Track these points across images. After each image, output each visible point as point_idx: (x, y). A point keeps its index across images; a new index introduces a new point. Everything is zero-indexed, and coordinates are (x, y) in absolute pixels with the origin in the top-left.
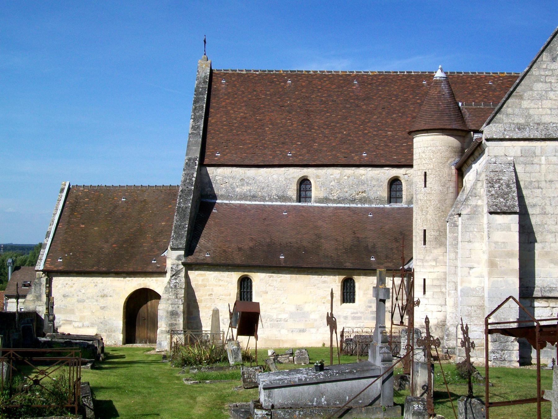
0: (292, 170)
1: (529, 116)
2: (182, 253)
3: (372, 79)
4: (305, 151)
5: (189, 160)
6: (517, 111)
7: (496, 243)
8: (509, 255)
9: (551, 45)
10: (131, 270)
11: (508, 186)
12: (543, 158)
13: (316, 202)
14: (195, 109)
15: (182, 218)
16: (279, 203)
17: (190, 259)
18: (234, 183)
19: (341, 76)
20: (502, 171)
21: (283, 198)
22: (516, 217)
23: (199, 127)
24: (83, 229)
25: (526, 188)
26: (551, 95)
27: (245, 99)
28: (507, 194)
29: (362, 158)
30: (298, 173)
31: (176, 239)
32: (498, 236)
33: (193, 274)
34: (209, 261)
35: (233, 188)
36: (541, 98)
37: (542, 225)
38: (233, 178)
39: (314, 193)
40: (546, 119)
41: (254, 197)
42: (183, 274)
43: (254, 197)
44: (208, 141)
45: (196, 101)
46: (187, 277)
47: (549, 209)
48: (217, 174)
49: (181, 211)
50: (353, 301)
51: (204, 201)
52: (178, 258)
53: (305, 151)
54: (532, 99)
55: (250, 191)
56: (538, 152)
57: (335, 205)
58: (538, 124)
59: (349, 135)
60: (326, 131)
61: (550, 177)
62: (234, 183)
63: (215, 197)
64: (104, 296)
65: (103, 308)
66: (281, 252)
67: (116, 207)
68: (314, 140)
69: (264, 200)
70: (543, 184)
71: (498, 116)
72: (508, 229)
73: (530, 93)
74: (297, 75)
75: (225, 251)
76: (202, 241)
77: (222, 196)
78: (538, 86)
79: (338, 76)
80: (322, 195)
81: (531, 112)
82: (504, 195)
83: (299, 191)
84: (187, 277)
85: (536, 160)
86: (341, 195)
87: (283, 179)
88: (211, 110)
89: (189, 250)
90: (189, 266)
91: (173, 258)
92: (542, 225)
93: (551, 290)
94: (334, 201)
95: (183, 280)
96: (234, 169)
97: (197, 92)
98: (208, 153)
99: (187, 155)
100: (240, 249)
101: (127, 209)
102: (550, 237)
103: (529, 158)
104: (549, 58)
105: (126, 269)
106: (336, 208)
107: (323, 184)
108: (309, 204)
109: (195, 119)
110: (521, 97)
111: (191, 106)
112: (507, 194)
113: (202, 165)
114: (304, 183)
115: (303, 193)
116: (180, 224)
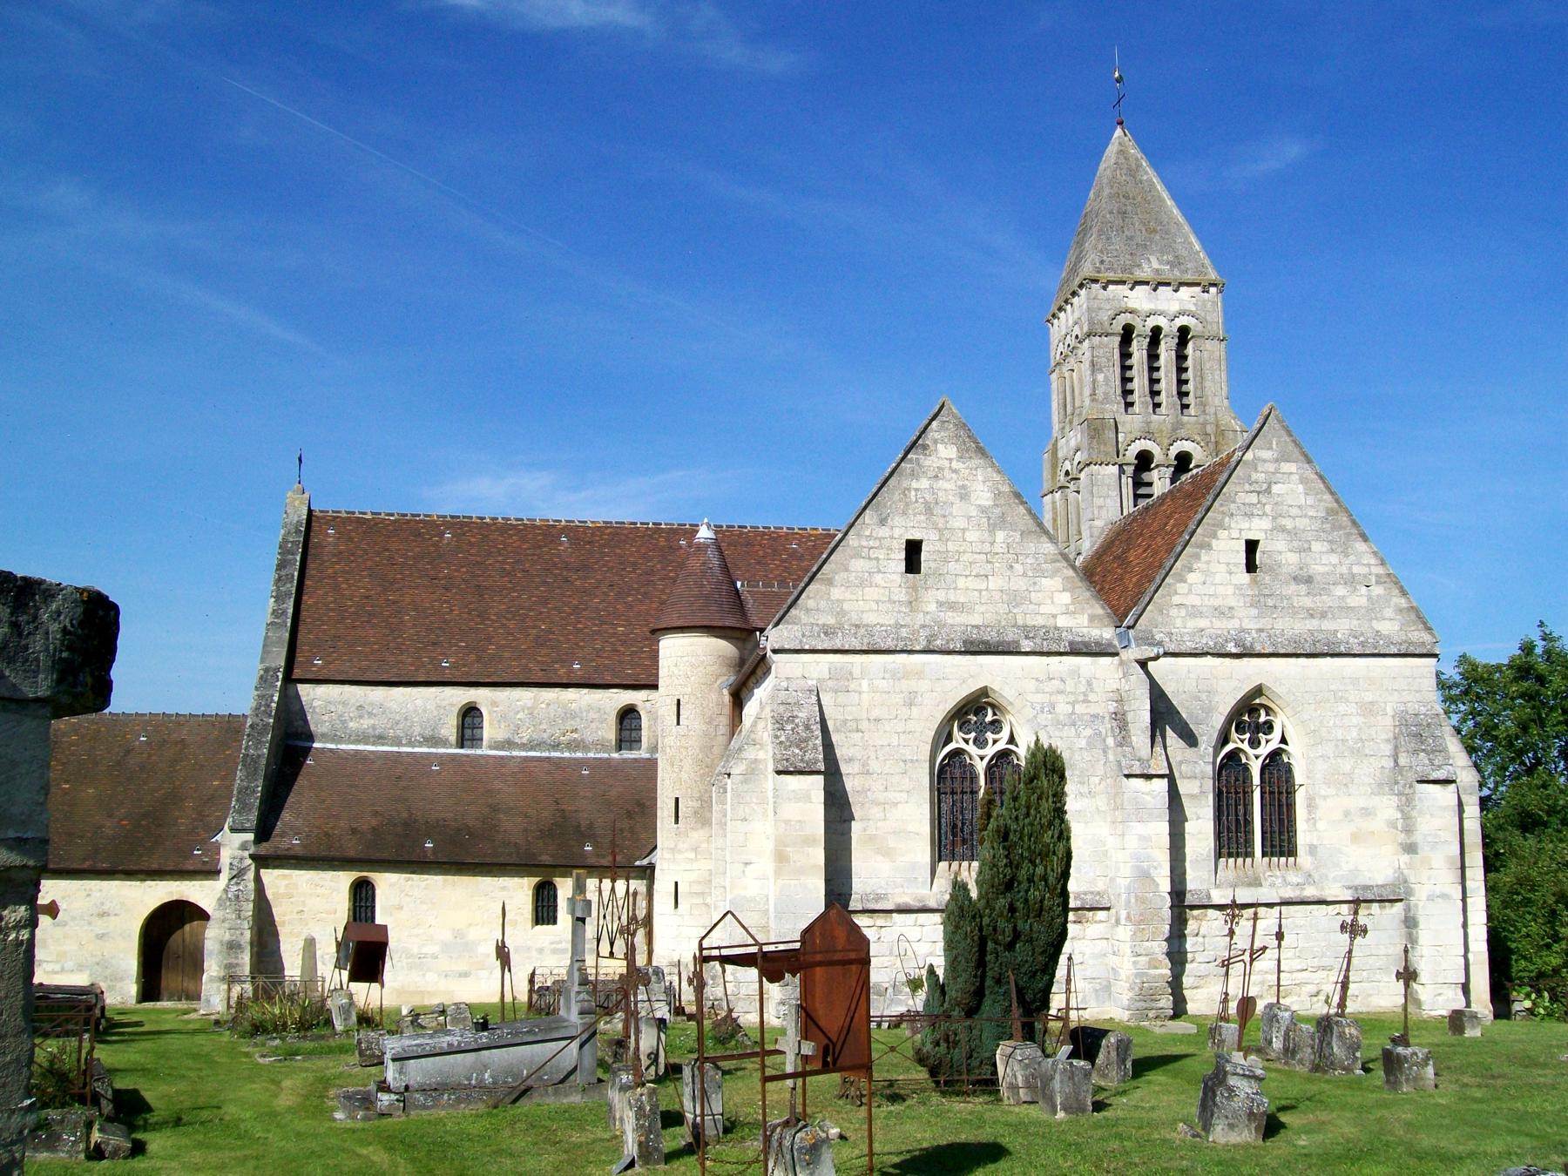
0: (449, 691)
1: (843, 613)
2: (251, 836)
3: (593, 534)
4: (473, 657)
5: (266, 670)
6: (823, 604)
7: (787, 822)
8: (809, 841)
9: (878, 498)
10: (155, 866)
11: (807, 727)
12: (865, 683)
13: (491, 747)
14: (279, 579)
15: (250, 776)
16: (424, 750)
17: (265, 848)
18: (344, 713)
19: (539, 528)
20: (797, 704)
23: (284, 612)
24: (65, 792)
25: (838, 731)
26: (878, 578)
27: (369, 563)
28: (806, 740)
29: (572, 671)
30: (459, 697)
31: (239, 812)
32: (791, 811)
33: (268, 875)
34: (300, 852)
36: (862, 584)
37: (864, 791)
38: (345, 704)
39: (489, 732)
40: (870, 618)
41: (380, 739)
42: (251, 875)
43: (380, 739)
44: (300, 636)
45: (281, 566)
46: (258, 880)
47: (874, 766)
48: (312, 695)
49: (251, 763)
50: (555, 923)
51: (291, 743)
52: (244, 847)
53: (473, 657)
54: (847, 585)
56: (856, 672)
57: (524, 754)
58: (857, 626)
59: (550, 631)
60: (511, 624)
61: (875, 713)
62: (344, 713)
63: (310, 737)
64: (103, 915)
65: (101, 937)
66: (429, 836)
67: (128, 752)
68: (489, 639)
69: (399, 744)
70: (864, 725)
71: (793, 612)
72: (808, 798)
73: (845, 575)
74: (463, 524)
75: (327, 834)
76: (286, 816)
77: (323, 735)
78: (858, 565)
79: (535, 527)
80: (501, 735)
81: (846, 606)
82: (801, 743)
83: (462, 727)
84: (258, 880)
85: (852, 686)
87: (434, 707)
88: (307, 582)
89: (263, 832)
90: (262, 861)
91: (232, 845)
92: (864, 791)
93: (878, 898)
94: (523, 747)
95: (251, 885)
96: (347, 688)
97: (284, 549)
98: (299, 658)
99: (262, 661)
100: (354, 831)
101: (150, 756)
102: (875, 812)
103: (842, 682)
104: (876, 519)
105: (145, 866)
106: (526, 759)
107: (504, 717)
108: (479, 752)
109: (279, 598)
110: (830, 582)
111: (272, 575)
112: (806, 740)
113: (290, 679)
114: (470, 714)
115: (468, 732)
116: (249, 785)
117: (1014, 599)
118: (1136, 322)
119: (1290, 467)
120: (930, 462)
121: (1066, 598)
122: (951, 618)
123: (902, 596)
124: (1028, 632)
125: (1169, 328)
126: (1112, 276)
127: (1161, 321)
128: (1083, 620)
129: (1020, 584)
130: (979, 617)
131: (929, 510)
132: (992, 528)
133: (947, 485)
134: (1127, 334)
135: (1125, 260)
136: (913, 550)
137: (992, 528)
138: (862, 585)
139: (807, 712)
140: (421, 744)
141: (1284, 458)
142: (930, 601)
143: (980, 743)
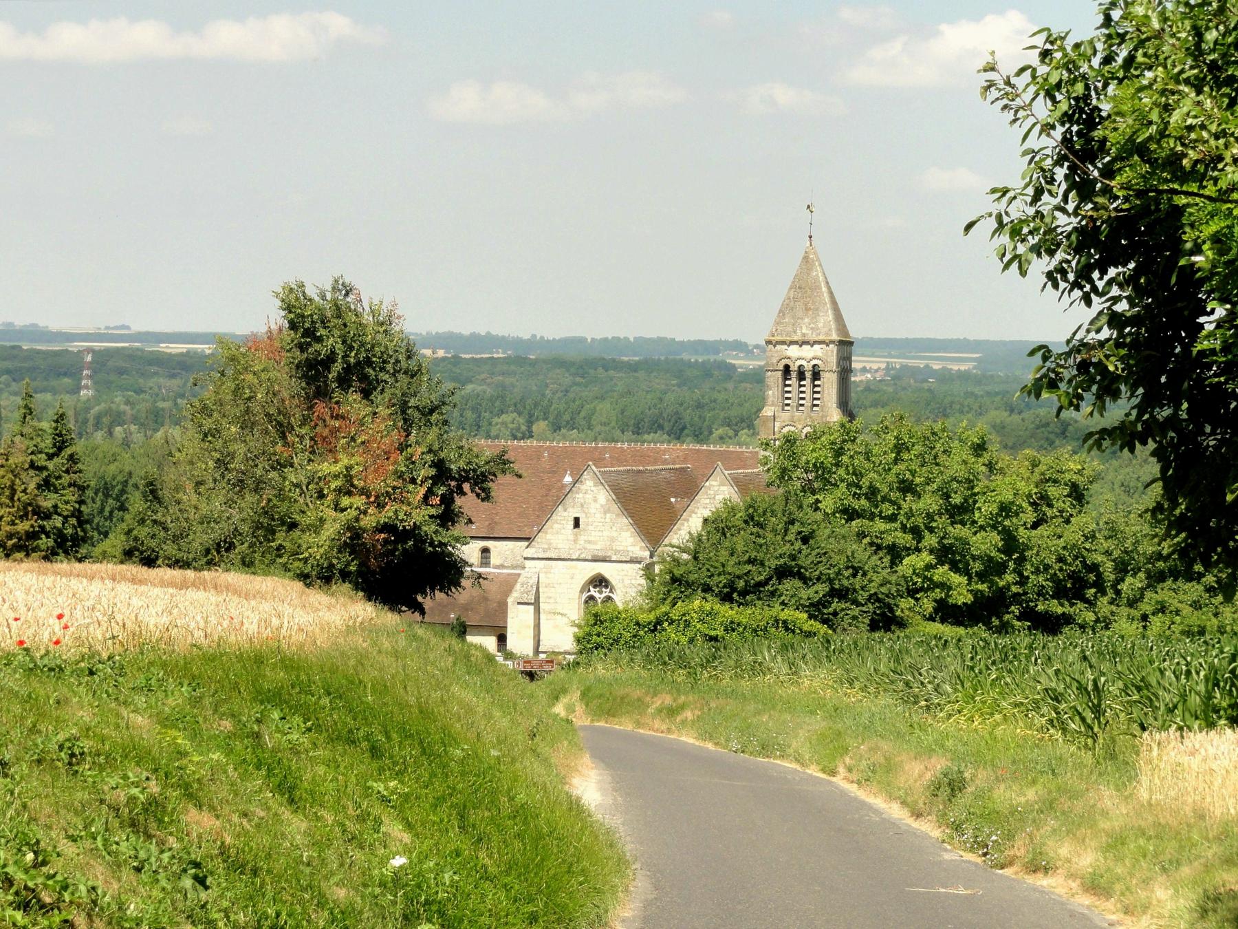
22: (532, 607)
39: (495, 559)
78: (556, 526)
106: (509, 574)
114: (485, 551)
117: (613, 540)
118: (791, 364)
119: (723, 488)
120: (584, 487)
121: (632, 540)
122: (589, 546)
123: (571, 537)
124: (617, 552)
125: (808, 367)
126: (779, 338)
127: (804, 363)
128: (637, 548)
129: (615, 534)
130: (598, 548)
131: (582, 506)
132: (605, 513)
133: (589, 497)
134: (787, 370)
135: (790, 329)
136: (577, 523)
137: (605, 513)
138: (558, 533)
139: (534, 580)
141: (722, 484)
142: (582, 540)
143: (601, 592)
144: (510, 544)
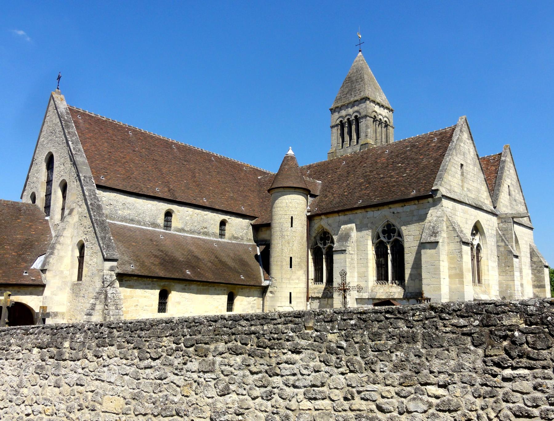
16: (150, 228)
21: (155, 225)
35: (116, 210)
41: (132, 221)
43: (132, 221)
50: (159, 312)
55: (129, 214)
69: (140, 225)
80: (180, 226)
86: (192, 228)
94: (187, 232)
140: (149, 226)
144: (190, 210)
